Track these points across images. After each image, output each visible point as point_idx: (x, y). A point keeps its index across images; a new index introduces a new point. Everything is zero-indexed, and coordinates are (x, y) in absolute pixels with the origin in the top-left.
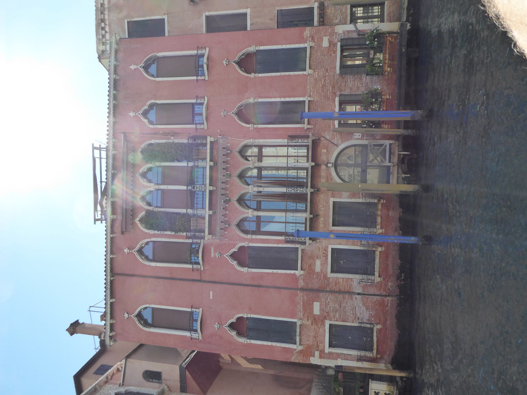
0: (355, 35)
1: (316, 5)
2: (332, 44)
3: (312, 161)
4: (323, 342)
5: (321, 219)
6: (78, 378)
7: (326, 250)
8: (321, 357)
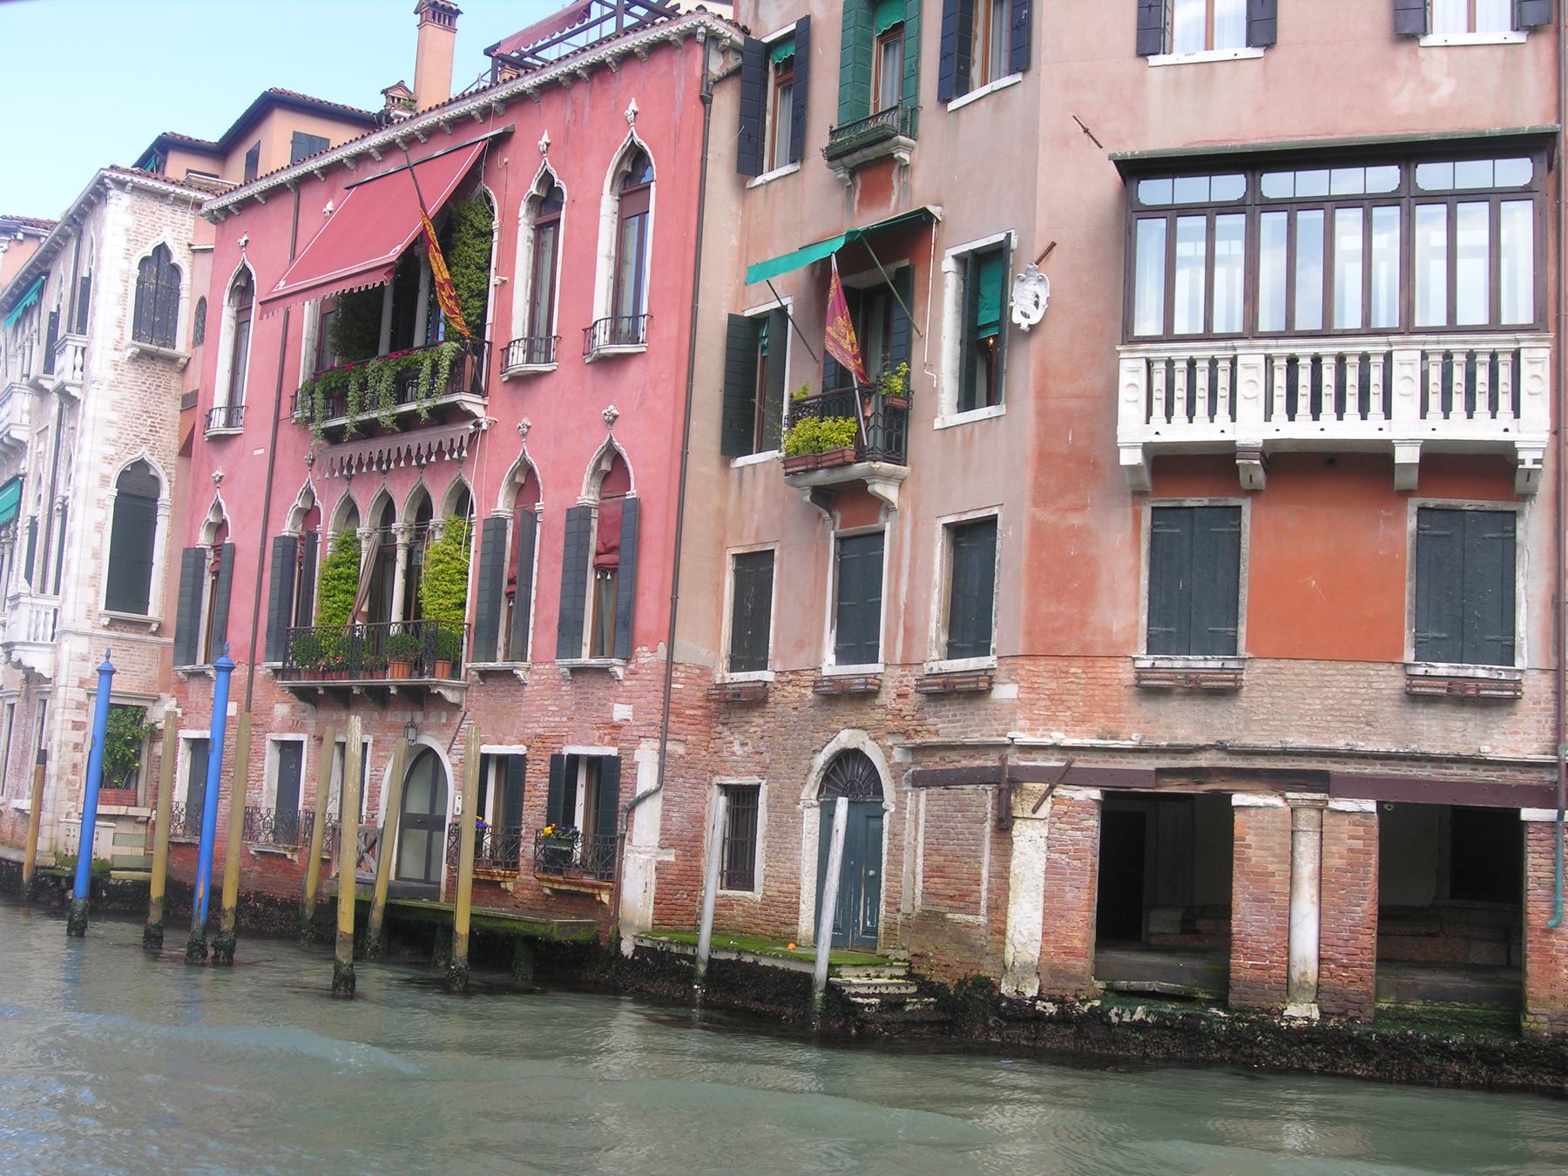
0: (624, 799)
1: (767, 675)
2: (615, 729)
6: (270, 103)
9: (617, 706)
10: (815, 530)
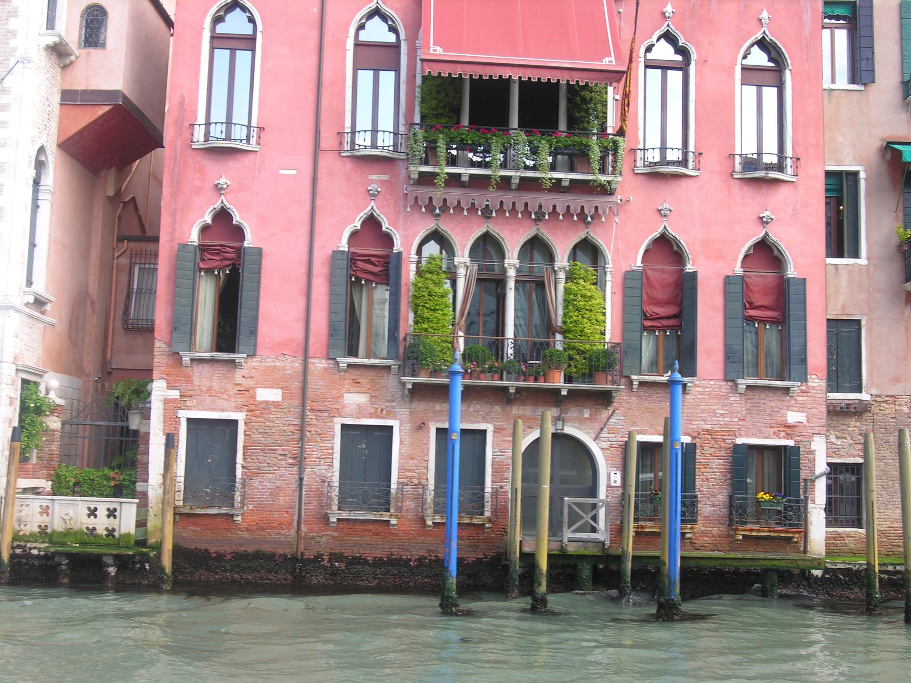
0: (804, 474)
1: (865, 396)
3: (570, 391)
4: (200, 407)
7: (390, 415)
8: (167, 401)
9: (789, 413)
10: (902, 313)
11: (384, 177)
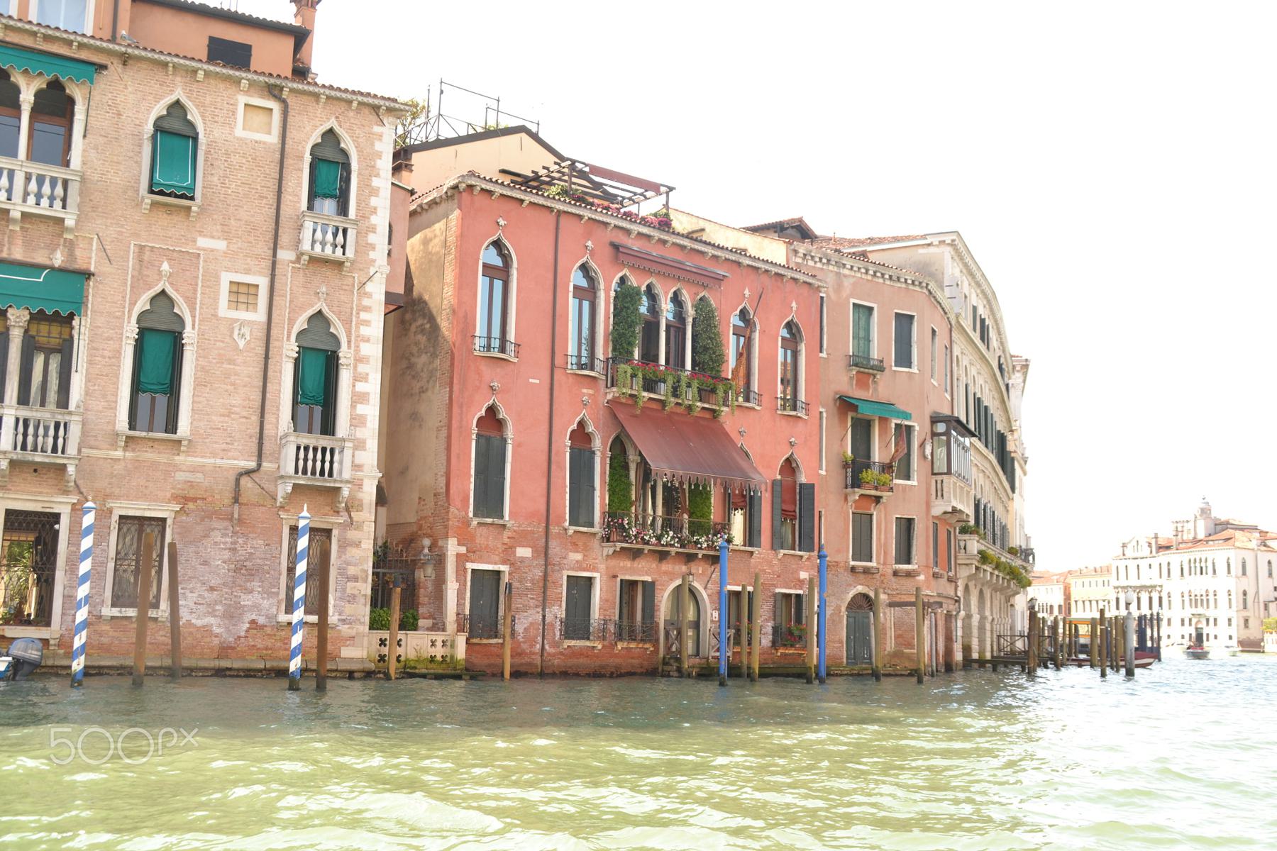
4: (481, 561)
5: (628, 564)
7: (595, 570)
8: (458, 556)
11: (591, 392)
